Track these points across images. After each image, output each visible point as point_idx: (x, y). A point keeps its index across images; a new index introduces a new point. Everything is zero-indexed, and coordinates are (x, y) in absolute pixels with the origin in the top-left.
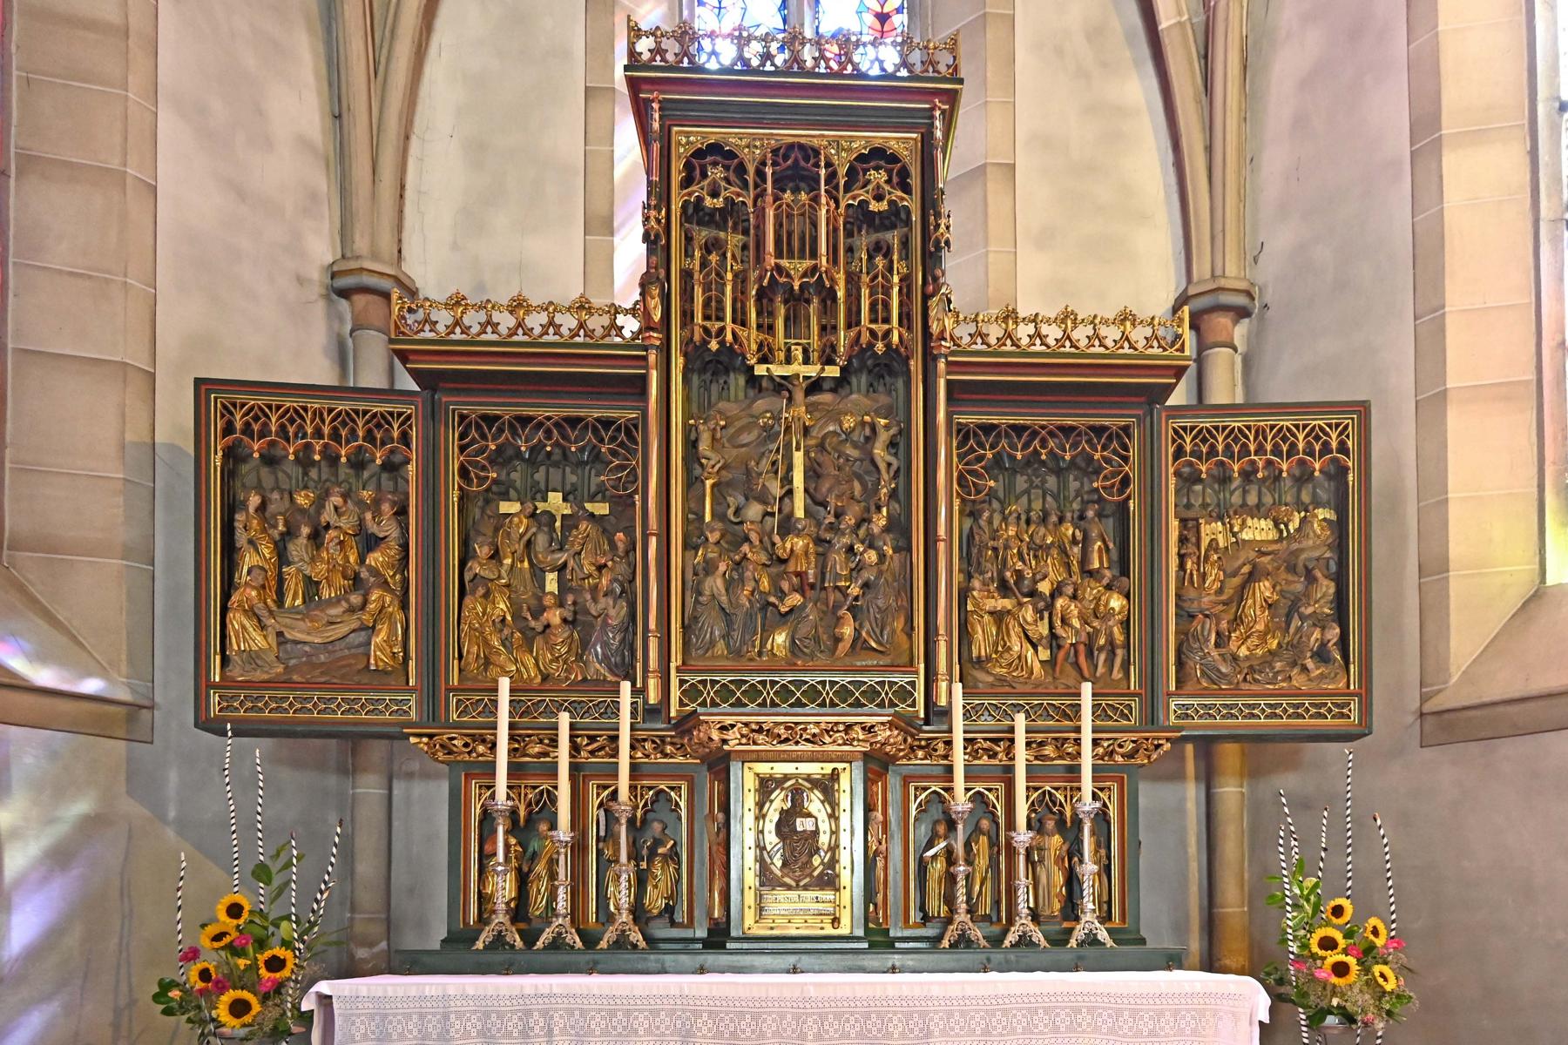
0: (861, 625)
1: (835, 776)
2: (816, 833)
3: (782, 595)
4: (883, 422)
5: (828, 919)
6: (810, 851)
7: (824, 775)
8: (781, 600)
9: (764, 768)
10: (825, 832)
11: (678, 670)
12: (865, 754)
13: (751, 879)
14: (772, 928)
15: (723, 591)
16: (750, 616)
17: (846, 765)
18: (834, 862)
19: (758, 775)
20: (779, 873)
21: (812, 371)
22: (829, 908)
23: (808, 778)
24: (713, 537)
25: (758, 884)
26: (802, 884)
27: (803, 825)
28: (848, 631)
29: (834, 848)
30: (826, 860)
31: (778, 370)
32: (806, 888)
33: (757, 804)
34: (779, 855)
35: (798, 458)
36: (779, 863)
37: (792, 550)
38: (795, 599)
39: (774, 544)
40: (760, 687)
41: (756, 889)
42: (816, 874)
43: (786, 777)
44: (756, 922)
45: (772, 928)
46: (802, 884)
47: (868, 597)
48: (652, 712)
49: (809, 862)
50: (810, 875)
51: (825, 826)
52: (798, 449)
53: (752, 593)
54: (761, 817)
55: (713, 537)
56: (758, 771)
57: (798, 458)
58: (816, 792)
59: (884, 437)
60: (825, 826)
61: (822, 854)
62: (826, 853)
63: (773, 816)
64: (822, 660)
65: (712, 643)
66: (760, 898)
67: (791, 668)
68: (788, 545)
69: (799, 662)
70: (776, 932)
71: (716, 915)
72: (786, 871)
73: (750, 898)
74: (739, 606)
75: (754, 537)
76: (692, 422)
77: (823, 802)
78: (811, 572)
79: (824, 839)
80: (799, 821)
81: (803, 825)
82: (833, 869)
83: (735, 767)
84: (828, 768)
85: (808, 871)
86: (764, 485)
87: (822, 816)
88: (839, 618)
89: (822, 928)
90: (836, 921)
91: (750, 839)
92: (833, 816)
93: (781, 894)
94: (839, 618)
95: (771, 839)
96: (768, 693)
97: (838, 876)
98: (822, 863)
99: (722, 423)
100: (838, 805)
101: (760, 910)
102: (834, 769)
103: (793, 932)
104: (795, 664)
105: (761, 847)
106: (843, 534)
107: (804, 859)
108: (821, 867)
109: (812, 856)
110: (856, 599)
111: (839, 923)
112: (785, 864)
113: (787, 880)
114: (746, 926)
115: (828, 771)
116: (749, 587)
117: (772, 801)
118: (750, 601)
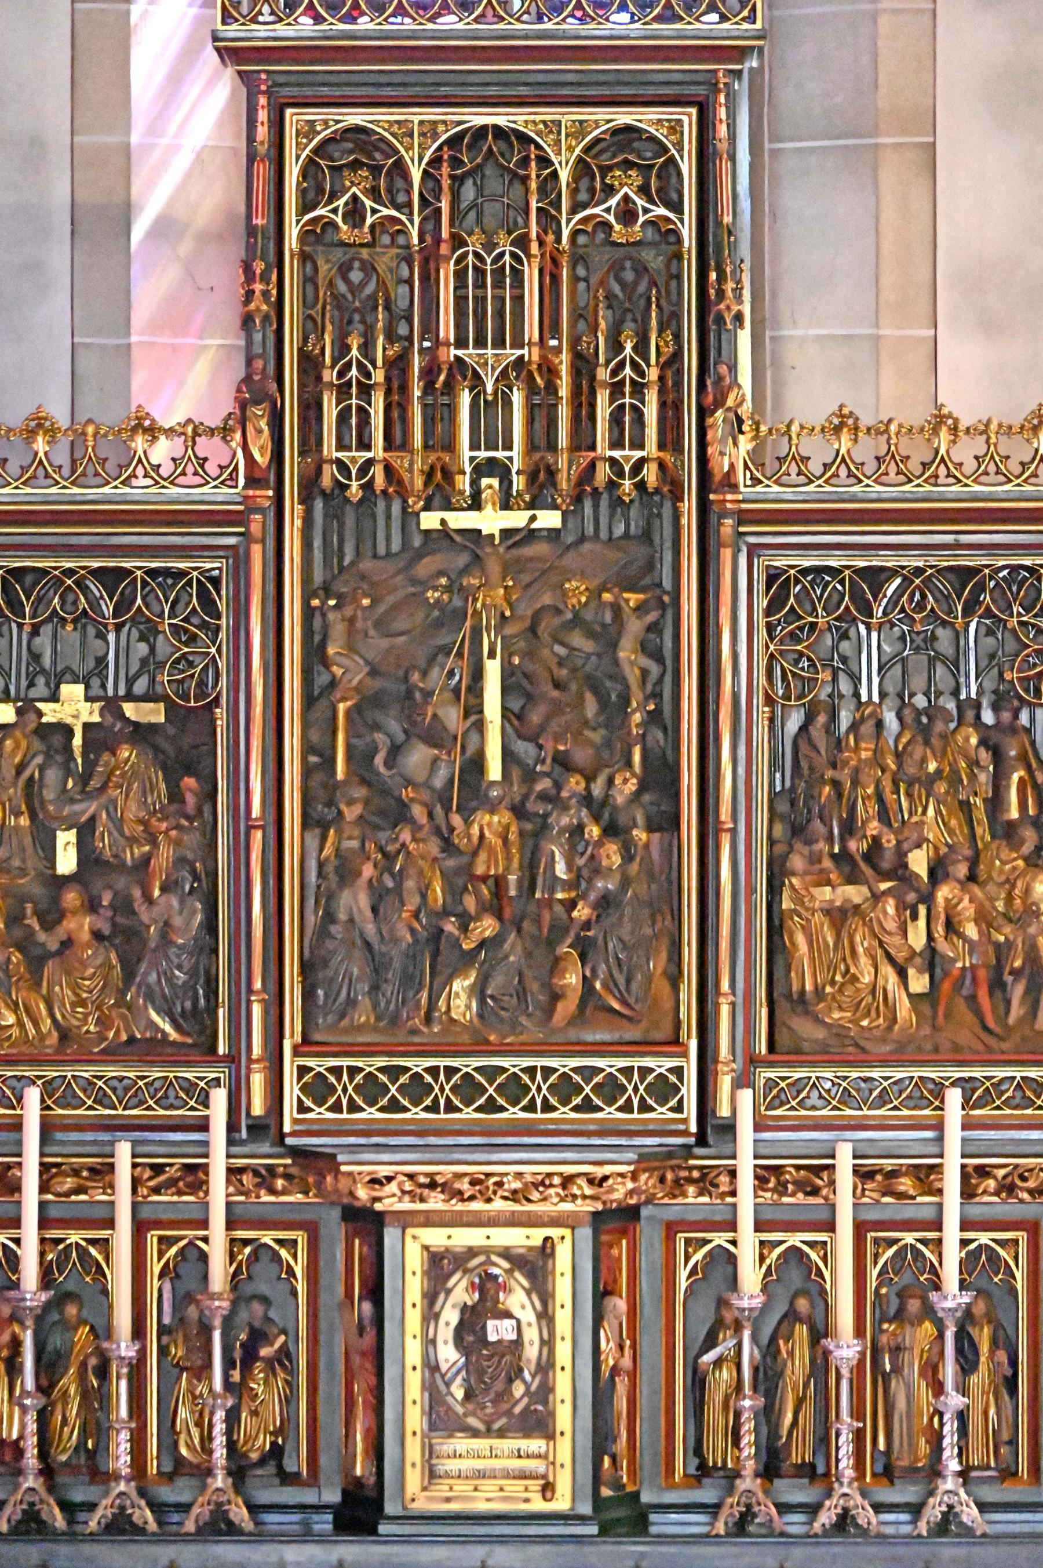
0: (594, 971)
1: (547, 1249)
2: (518, 1343)
3: (465, 923)
4: (633, 598)
5: (535, 1485)
6: (508, 1374)
7: (530, 1249)
8: (464, 928)
9: (436, 1237)
10: (531, 1344)
11: (296, 1052)
12: (596, 1214)
13: (415, 1419)
14: (448, 1500)
15: (369, 914)
16: (412, 956)
17: (567, 1232)
18: (546, 1390)
19: (426, 1248)
20: (460, 1410)
21: (517, 519)
22: (537, 1466)
23: (506, 1253)
24: (351, 813)
25: (425, 1427)
26: (496, 1426)
27: (498, 1330)
28: (572, 979)
29: (546, 1367)
30: (533, 1387)
31: (459, 520)
32: (501, 1434)
33: (424, 1295)
34: (459, 1380)
35: (493, 670)
36: (459, 1394)
37: (482, 836)
38: (487, 927)
39: (452, 829)
40: (428, 1079)
41: (423, 1436)
42: (517, 1410)
43: (472, 1252)
44: (424, 1489)
45: (448, 1500)
46: (496, 1426)
47: (606, 923)
48: (257, 1129)
49: (507, 1391)
50: (509, 1413)
51: (532, 1334)
52: (492, 655)
53: (416, 915)
54: (430, 1315)
55: (351, 813)
56: (427, 1243)
57: (493, 670)
58: (517, 1275)
59: (634, 627)
60: (532, 1334)
61: (527, 1376)
62: (533, 1377)
63: (451, 1316)
64: (532, 1031)
65: (351, 1002)
66: (430, 1453)
67: (480, 1046)
68: (475, 830)
69: (492, 1038)
70: (454, 1507)
71: (358, 1472)
72: (470, 1407)
73: (414, 1451)
74: (395, 940)
75: (418, 812)
76: (315, 602)
77: (528, 1293)
78: (512, 878)
79: (532, 1352)
80: (491, 1324)
81: (498, 1330)
82: (545, 1402)
83: (391, 1235)
84: (536, 1236)
85: (505, 1406)
86: (435, 716)
87: (528, 1317)
88: (557, 960)
89: (527, 1500)
90: (548, 1489)
91: (414, 1352)
92: (546, 1316)
93: (462, 1444)
94: (557, 960)
95: (448, 1354)
96: (442, 1089)
97: (552, 1414)
98: (527, 1392)
99: (366, 602)
100: (553, 1296)
101: (432, 1475)
102: (546, 1239)
103: (482, 1506)
104: (487, 1042)
105: (431, 1366)
106: (566, 808)
107: (499, 1386)
108: (526, 1400)
109: (510, 1381)
110: (587, 925)
111: (553, 1491)
112: (468, 1396)
113: (473, 1422)
114: (409, 1495)
115: (537, 1242)
116: (413, 902)
117: (448, 1292)
118: (413, 931)
